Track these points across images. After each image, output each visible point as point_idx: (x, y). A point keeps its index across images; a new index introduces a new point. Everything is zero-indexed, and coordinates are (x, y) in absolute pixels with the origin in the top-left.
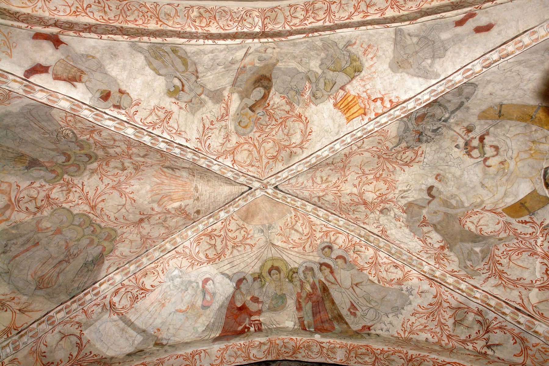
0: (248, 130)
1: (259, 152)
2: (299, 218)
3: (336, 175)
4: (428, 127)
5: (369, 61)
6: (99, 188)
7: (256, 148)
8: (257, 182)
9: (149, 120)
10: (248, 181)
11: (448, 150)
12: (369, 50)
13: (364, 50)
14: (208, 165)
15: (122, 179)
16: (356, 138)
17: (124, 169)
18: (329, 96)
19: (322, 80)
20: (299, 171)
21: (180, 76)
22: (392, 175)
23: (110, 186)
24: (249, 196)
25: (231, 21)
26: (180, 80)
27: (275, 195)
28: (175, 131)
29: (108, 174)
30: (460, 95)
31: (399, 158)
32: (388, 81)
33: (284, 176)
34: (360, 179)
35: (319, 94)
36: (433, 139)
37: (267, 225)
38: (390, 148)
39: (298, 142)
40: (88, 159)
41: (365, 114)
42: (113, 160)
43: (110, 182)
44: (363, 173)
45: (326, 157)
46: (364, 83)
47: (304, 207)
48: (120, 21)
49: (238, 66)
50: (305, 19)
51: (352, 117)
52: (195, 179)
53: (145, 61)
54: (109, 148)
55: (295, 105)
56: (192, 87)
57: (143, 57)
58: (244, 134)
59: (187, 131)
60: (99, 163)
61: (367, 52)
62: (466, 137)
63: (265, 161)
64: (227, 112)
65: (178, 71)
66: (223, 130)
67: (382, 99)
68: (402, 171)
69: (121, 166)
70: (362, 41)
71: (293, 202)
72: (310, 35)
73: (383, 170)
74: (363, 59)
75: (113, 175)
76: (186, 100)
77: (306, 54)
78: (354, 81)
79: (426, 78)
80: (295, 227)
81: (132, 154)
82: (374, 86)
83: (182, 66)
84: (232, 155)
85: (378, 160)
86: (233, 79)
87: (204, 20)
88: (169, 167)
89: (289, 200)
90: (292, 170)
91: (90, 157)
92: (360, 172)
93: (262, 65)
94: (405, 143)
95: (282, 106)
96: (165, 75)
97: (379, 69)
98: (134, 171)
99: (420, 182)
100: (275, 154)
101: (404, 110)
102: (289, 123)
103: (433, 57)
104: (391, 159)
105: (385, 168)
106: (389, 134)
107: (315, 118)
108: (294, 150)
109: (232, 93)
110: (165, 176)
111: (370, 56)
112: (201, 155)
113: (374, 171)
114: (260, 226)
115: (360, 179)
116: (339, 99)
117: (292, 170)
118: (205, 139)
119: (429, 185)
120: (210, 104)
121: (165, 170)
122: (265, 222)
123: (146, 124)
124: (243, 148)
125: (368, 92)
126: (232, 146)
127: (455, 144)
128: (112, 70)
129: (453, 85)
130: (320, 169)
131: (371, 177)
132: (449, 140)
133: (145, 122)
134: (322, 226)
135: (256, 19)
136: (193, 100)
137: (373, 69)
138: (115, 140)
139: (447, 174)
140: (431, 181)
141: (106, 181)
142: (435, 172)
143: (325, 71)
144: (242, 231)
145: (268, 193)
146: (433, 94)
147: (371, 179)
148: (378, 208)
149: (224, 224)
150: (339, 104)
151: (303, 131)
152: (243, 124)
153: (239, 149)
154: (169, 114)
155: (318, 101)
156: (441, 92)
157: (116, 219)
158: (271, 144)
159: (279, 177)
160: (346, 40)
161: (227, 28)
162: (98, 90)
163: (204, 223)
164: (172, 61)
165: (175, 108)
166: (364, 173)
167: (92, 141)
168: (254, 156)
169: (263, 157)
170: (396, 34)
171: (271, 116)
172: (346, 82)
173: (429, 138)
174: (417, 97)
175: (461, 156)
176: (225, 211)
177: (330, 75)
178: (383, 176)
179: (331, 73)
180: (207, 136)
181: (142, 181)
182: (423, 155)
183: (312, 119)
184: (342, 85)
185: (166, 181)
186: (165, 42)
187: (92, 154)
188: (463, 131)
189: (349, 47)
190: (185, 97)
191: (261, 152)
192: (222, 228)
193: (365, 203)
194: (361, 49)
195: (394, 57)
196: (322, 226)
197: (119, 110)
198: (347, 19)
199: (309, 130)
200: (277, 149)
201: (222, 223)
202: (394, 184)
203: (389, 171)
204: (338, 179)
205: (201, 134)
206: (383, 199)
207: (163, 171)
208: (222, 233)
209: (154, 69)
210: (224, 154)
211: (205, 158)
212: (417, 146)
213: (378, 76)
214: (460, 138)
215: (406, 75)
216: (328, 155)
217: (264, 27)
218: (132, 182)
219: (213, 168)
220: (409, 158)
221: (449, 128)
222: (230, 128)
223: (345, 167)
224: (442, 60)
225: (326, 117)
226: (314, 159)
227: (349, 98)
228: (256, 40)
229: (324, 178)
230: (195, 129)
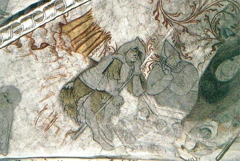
5: (50, 104)
12: (48, 122)
13: (56, 123)
18: (116, 52)
19: (124, 78)
32: (22, 75)
35: (131, 56)
41: (61, 25)
46: (60, 70)
51: (83, 20)
55: (171, 41)
61: (51, 118)
67: (33, 47)
70: (57, 138)
74: (58, 108)
77: (140, 127)
78: (75, 73)
82: (45, 66)
93: (208, 120)
95: (192, 43)
97: (36, 92)
102: (185, 11)
107: (143, 19)
111: (47, 112)
125: (54, 58)
137: (45, 92)
143: (117, 92)
150: (101, 39)
155: (134, 45)
160: (78, 141)
171: (214, 26)
177: (109, 87)
179: (108, 89)
183: (147, 16)
184: (95, 68)
189: (76, 128)
194: (59, 125)
195: (13, 110)
225: (125, 19)
227: (86, 48)
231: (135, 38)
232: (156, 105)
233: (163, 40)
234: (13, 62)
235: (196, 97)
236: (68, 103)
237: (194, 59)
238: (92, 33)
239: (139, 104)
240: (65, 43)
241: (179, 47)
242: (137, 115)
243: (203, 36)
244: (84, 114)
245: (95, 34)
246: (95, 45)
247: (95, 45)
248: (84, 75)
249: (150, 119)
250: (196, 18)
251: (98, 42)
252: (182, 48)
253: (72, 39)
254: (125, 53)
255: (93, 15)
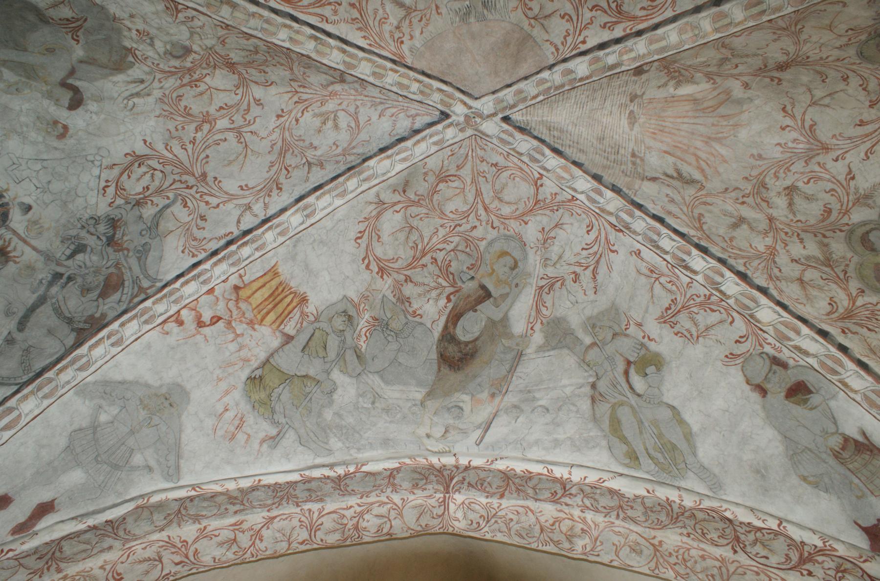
0: (497, 247)
1: (478, 193)
2: (392, 36)
3: (301, 132)
4: (95, 258)
6: (862, 155)
7: (483, 202)
8: (490, 133)
9: (714, 318)
10: (510, 139)
11: (47, 198)
12: (232, 429)
14: (600, 194)
15: (799, 166)
16: (253, 241)
17: (791, 190)
18: (317, 319)
19: (332, 354)
20: (388, 157)
21: (629, 395)
22: (173, 130)
23: (834, 154)
24: (511, 102)
25: (512, 520)
26: (631, 387)
27: (446, 99)
28: (662, 280)
29: (830, 186)
30: (27, 351)
31: (158, 174)
33: (423, 146)
34: (248, 117)
35: (339, 323)
36: (83, 227)
37: (472, 20)
38: (180, 201)
39: (388, 215)
40: (872, 237)
41: (237, 288)
42: (813, 221)
43: (830, 164)
44: (240, 133)
45: (324, 194)
47: (377, 70)
48: (736, 564)
49: (506, 398)
50: (361, 515)
51: (267, 278)
52: (632, 145)
53: (698, 445)
54: (817, 259)
55: (391, 297)
56: (606, 365)
57: (701, 453)
58: (507, 238)
59: (634, 274)
60: (845, 220)
61: (237, 422)
62: (8, 236)
63: (466, 172)
64: (540, 295)
65: (632, 407)
66: (554, 257)
67: (200, 324)
68: (149, 140)
69: (798, 200)
71: (405, 81)
72: (352, 469)
73: (193, 142)
74: (245, 407)
75: (820, 179)
76: (626, 340)
78: (263, 356)
79: (106, 383)
80: (403, 13)
81: (766, 233)
83: (623, 420)
84: (540, 197)
85: (208, 169)
86: (518, 370)
87: (564, 529)
88: (687, 182)
89: (415, 87)
90: (404, 160)
91: (865, 240)
92: (248, 136)
94: (145, 216)
95: (420, 295)
96: (661, 403)
98: (767, 180)
99: (103, 116)
100: (442, 186)
101: (146, 317)
102: (405, 254)
103: (94, 427)
104: (176, 171)
105: (190, 147)
106: (181, 243)
108: (397, 197)
109: (525, 337)
110: (698, 158)
112: (613, 220)
113: (217, 137)
114: (490, 17)
115: (248, 117)
116: (296, 314)
117: (404, 160)
118: (595, 248)
119: (80, 110)
120: (575, 321)
121: (697, 176)
122: (476, 26)
123: (722, 310)
124: (513, 207)
125: (231, 336)
126: (539, 218)
127: (31, 213)
128: (770, 441)
129: (39, 389)
130: (339, 150)
131: (223, 123)
132: (46, 226)
133: (724, 316)
134: (333, 18)
135: (459, 515)
136: (609, 337)
137: (223, 386)
138: (801, 280)
139: (40, 139)
140: (77, 120)
141: (839, 169)
142: (70, 142)
144: (536, 10)
145: (465, 104)
146: (84, 360)
147: (223, 117)
148: (197, 57)
149: (581, 39)
150: (294, 304)
151: (375, 238)
152: (509, 261)
153: (521, 208)
154: (668, 318)
155: (341, 307)
156: (65, 368)
157: (845, 79)
158: (450, 207)
159: (435, 143)
161: (521, 510)
162: (811, 409)
163: (633, 55)
164: (641, 433)
165: (653, 328)
166: (239, 134)
167: (854, 285)
168: (489, 186)
169: (469, 181)
170: (178, 468)
171: (445, 271)
172: (281, 353)
173: (92, 230)
174: (120, 348)
175: (12, 185)
176: (573, 76)
177: (314, 369)
178: (192, 127)
179: (312, 373)
180: (591, 251)
181: (755, 152)
182: (103, 184)
184: (290, 345)
185: (699, 144)
186: (650, 487)
187: (860, 248)
188: (15, 249)
189: (274, 432)
190: (626, 347)
191: (474, 192)
192: (585, 28)
193: (231, 66)
194: (249, 431)
195: (179, 416)
196: (333, 18)
197: (777, 354)
198: (275, 517)
199: (364, 242)
200: (436, 197)
201: (584, 42)
202: (166, 108)
203: (180, 138)
204: (297, 120)
205: (603, 259)
206: (188, 76)
207: (702, 171)
208: (588, 15)
209: (681, 422)
210: (555, 205)
211: (603, 210)
212: (119, 207)
213: (212, 373)
214: (21, 231)
215: (151, 381)
216: (318, 198)
217: (444, 501)
218: (777, 154)
219: (589, 185)
220: (134, 176)
221: (48, 257)
222: (538, 258)
223: (282, 153)
224: (76, 426)
226: (350, 188)
227: (274, 318)
228: (464, 461)
229: (330, 124)
230: (614, 274)
231: (341, 297)
232: (382, 384)
233: (380, 296)
234: (173, 348)
235: (435, 367)
236: (257, 398)
237: (424, 317)
238: (281, 296)
239: (358, 388)
240: (244, 314)
241: (403, 303)
242: (358, 402)
243: (433, 284)
244: (282, 410)
245: (286, 297)
246: (286, 312)
247: (286, 312)
248: (276, 356)
249: (377, 405)
250: (421, 263)
251: (290, 308)
252: (407, 304)
253: (254, 306)
254: (331, 320)
255: (280, 270)
